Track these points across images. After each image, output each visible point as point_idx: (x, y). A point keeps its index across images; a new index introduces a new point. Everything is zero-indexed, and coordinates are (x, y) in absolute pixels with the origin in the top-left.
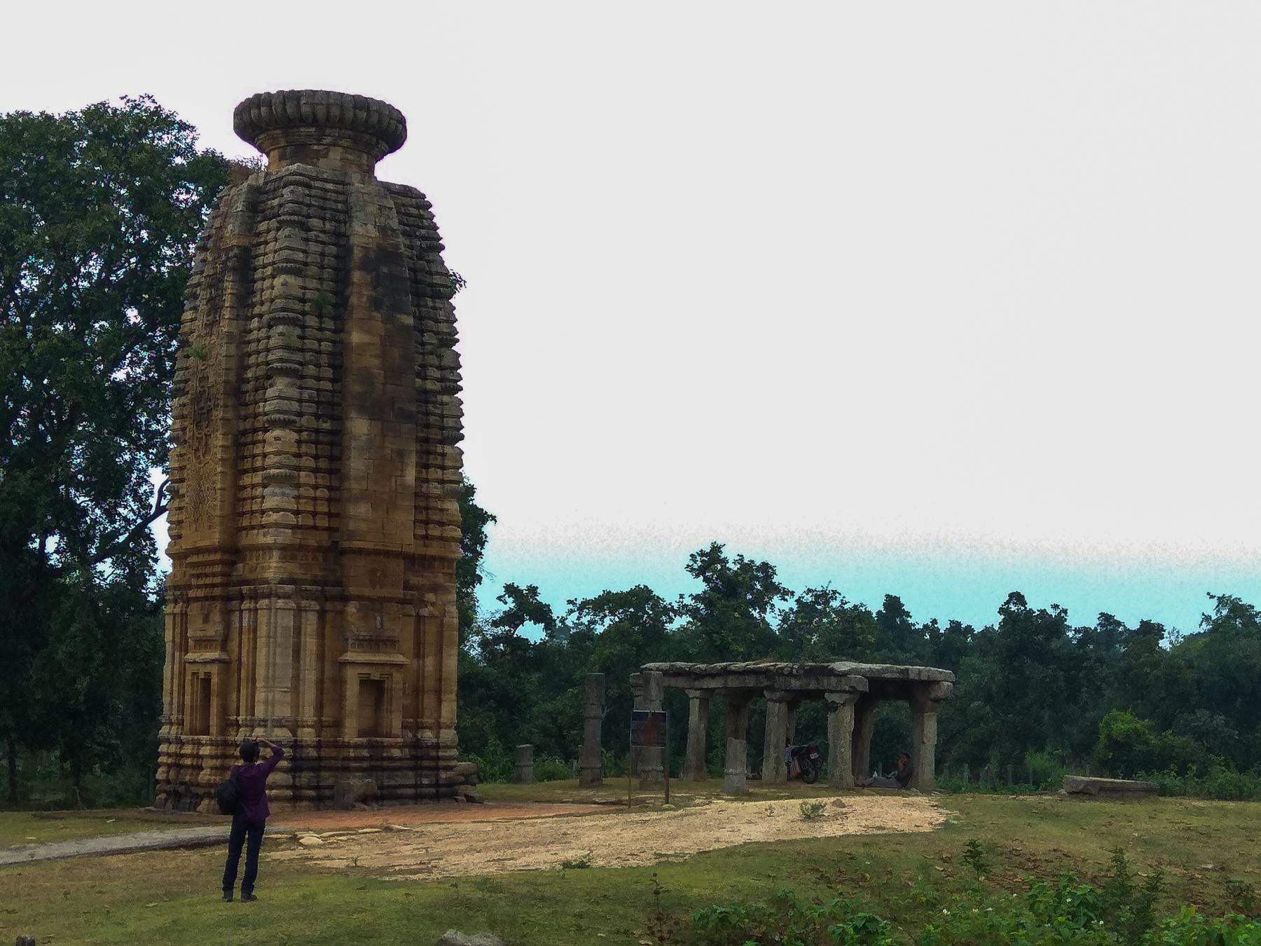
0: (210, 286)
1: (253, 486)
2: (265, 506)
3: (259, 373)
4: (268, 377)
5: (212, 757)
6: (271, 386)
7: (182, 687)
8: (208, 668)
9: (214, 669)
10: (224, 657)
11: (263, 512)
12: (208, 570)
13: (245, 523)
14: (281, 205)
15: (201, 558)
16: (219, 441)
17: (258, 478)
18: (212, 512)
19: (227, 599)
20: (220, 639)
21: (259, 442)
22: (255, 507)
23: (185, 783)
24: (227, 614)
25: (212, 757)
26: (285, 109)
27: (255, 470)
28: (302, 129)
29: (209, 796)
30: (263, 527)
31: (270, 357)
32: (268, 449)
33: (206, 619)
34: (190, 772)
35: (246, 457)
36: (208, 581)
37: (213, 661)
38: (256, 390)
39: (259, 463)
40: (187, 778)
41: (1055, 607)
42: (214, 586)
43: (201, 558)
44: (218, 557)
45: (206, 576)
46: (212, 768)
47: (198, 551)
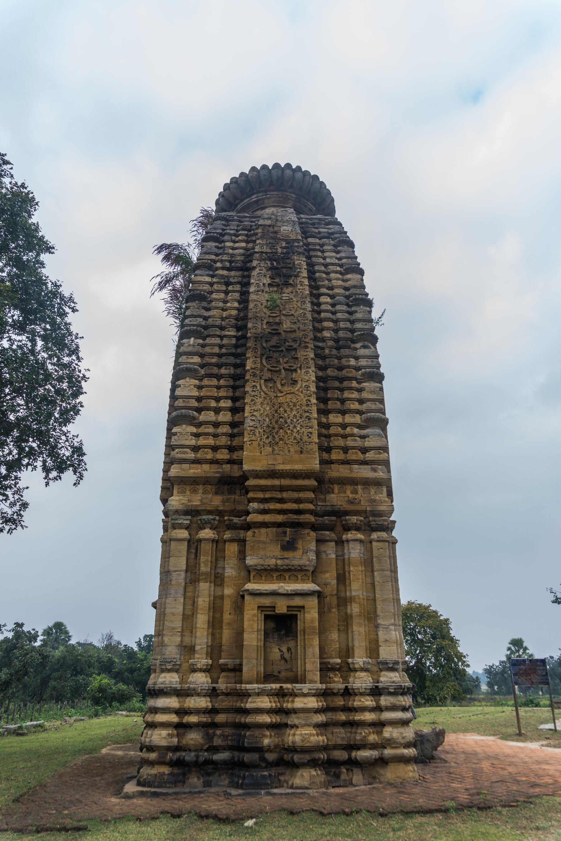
0: (271, 259)
1: (344, 426)
2: (368, 443)
3: (341, 334)
4: (353, 342)
5: (317, 711)
6: (365, 347)
7: (215, 624)
8: (297, 601)
9: (313, 602)
10: (317, 588)
11: (364, 450)
12: (285, 495)
13: (335, 456)
14: (328, 233)
15: (277, 482)
16: (308, 377)
17: (357, 419)
18: (305, 438)
19: (314, 527)
20: (311, 569)
21: (351, 388)
22: (350, 442)
23: (260, 750)
24: (320, 541)
25: (317, 711)
26: (312, 184)
27: (343, 413)
28: (309, 204)
29: (313, 763)
30: (364, 463)
31: (358, 325)
32: (365, 395)
33: (289, 546)
34: (268, 733)
35: (329, 399)
36: (294, 506)
37: (311, 594)
38: (338, 348)
39: (355, 406)
40: (266, 741)
41: (34, 629)
42: (299, 512)
43: (277, 482)
44: (313, 482)
45: (281, 501)
46: (317, 726)
47: (272, 474)
